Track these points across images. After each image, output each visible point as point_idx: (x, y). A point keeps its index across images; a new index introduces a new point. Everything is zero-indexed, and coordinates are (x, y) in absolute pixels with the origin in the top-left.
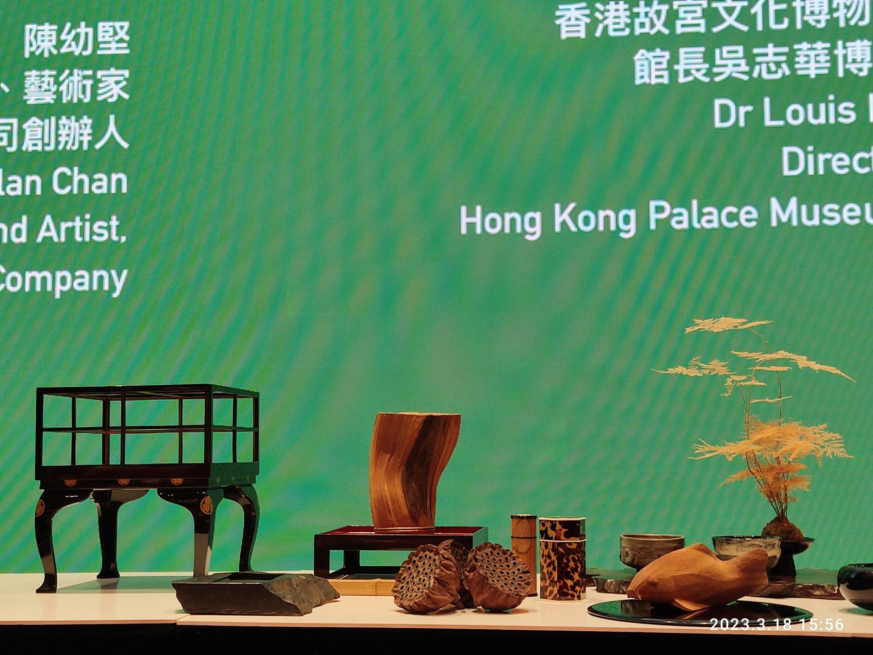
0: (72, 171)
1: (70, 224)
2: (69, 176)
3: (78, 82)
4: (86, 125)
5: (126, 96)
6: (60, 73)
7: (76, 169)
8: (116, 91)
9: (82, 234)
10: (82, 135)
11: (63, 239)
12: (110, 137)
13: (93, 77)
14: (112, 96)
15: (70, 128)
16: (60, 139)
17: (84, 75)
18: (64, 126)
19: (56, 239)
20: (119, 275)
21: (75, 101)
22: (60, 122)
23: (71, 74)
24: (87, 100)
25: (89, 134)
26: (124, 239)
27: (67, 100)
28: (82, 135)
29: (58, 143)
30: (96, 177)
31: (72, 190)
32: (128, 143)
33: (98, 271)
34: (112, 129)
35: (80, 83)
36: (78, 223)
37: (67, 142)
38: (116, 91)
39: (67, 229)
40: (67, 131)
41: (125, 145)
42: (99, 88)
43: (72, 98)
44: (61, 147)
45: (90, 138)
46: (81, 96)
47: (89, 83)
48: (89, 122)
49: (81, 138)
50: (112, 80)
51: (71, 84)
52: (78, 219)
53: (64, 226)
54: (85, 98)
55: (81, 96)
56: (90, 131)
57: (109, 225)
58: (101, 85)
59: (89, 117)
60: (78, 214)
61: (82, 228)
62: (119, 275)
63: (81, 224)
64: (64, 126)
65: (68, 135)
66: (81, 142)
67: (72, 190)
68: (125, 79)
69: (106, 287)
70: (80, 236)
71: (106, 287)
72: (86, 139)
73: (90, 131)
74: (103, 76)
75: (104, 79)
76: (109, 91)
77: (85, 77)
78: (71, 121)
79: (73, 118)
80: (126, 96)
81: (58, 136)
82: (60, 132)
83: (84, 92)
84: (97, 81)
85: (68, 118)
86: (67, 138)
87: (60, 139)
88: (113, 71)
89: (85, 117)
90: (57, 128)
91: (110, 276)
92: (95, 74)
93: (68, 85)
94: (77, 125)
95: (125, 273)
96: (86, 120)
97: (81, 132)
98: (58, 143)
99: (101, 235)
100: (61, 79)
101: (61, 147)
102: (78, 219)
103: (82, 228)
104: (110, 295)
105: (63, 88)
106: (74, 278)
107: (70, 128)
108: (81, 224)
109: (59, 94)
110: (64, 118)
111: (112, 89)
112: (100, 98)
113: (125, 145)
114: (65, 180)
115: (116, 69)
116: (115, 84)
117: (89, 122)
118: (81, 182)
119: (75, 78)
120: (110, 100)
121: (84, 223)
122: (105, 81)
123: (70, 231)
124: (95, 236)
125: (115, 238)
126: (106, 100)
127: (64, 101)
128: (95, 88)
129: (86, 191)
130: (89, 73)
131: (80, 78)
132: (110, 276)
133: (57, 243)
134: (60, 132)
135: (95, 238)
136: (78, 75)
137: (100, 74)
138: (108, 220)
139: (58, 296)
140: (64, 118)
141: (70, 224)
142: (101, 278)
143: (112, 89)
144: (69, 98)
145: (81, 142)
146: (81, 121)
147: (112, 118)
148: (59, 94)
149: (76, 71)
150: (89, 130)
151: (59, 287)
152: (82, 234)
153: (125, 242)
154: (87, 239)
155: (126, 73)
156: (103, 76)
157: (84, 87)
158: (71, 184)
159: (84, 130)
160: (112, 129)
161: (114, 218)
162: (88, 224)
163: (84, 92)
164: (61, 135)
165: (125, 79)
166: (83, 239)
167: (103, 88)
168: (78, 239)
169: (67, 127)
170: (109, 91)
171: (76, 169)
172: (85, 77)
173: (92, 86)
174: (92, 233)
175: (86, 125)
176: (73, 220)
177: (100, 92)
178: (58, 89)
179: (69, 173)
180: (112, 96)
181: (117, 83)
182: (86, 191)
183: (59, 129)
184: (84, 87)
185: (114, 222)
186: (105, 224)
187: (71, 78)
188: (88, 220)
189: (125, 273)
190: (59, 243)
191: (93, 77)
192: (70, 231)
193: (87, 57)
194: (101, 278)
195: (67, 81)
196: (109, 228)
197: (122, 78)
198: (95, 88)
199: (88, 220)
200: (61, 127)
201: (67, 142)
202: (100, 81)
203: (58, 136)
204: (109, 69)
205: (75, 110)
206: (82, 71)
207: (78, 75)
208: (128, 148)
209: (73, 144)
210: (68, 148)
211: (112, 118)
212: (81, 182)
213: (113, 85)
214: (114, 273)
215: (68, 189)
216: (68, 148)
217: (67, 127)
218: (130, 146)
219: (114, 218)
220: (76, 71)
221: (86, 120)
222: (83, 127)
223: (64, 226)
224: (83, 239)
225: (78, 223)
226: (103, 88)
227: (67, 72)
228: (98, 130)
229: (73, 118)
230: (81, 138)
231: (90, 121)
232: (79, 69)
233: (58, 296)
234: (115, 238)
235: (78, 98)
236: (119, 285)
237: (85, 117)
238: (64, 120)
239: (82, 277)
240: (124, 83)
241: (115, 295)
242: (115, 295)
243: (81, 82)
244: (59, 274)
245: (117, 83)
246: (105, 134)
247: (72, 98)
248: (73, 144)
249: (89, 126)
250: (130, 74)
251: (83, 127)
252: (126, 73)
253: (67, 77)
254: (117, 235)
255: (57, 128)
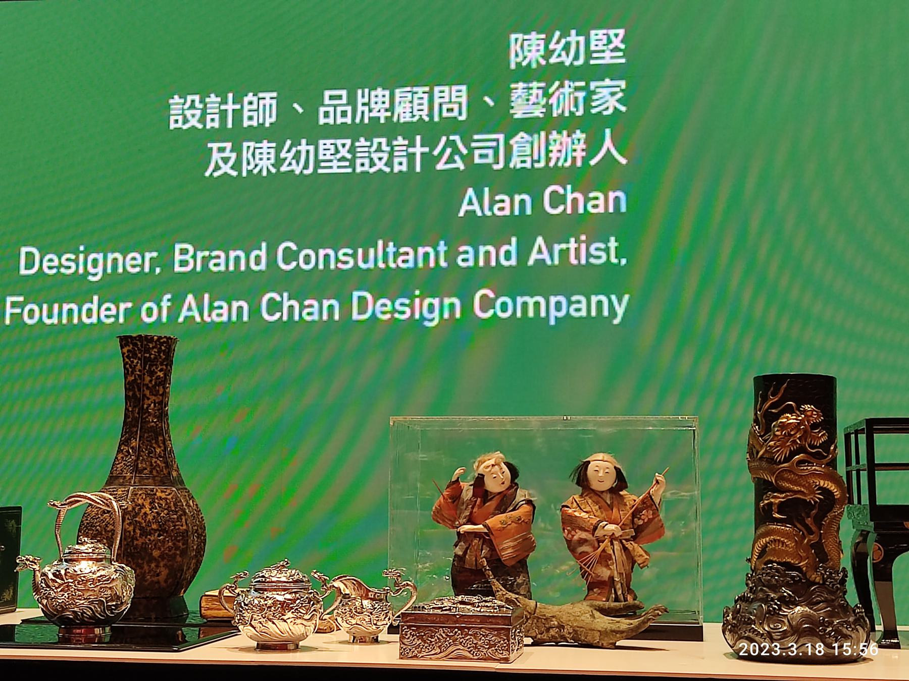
0: (565, 189)
1: (564, 246)
2: (562, 195)
3: (570, 94)
4: (579, 140)
5: (623, 109)
6: (549, 85)
7: (569, 187)
8: (612, 103)
9: (578, 257)
10: (575, 150)
11: (556, 262)
12: (606, 153)
13: (586, 88)
14: (607, 108)
15: (561, 143)
16: (551, 155)
17: (575, 86)
18: (555, 141)
19: (549, 262)
20: (620, 301)
21: (567, 114)
22: (550, 137)
23: (562, 86)
24: (580, 113)
25: (583, 150)
26: (624, 261)
27: (557, 114)
28: (575, 150)
29: (548, 160)
30: (592, 195)
31: (565, 210)
32: (627, 159)
33: (596, 296)
34: (608, 143)
35: (572, 96)
36: (572, 245)
37: (558, 159)
38: (612, 103)
39: (561, 251)
40: (558, 147)
41: (623, 161)
42: (593, 101)
43: (563, 112)
44: (552, 164)
45: (584, 154)
46: (573, 109)
47: (581, 95)
48: (583, 136)
49: (574, 154)
50: (606, 92)
51: (561, 97)
52: (572, 240)
53: (557, 248)
54: (577, 111)
55: (573, 109)
56: (584, 147)
57: (607, 246)
58: (594, 97)
59: (582, 132)
60: (572, 236)
61: (577, 250)
62: (620, 301)
63: (576, 245)
64: (555, 141)
65: (560, 151)
66: (574, 159)
67: (565, 210)
68: (622, 90)
69: (606, 313)
70: (576, 258)
71: (606, 313)
72: (579, 155)
73: (584, 147)
74: (597, 87)
75: (598, 90)
76: (604, 103)
77: (577, 89)
78: (563, 136)
79: (565, 133)
80: (623, 109)
81: (548, 152)
82: (550, 148)
83: (576, 106)
84: (590, 93)
85: (559, 132)
86: (559, 154)
87: (551, 155)
88: (608, 82)
89: (578, 132)
90: (548, 143)
91: (610, 301)
92: (588, 85)
93: (558, 98)
94: (569, 140)
95: (626, 298)
96: (578, 134)
97: (574, 147)
98: (548, 160)
99: (599, 257)
100: (551, 91)
101: (552, 164)
102: (572, 240)
103: (577, 250)
104: (611, 322)
105: (553, 101)
106: (570, 303)
107: (561, 143)
108: (576, 245)
109: (549, 107)
110: (554, 132)
111: (607, 101)
112: (594, 111)
113: (623, 161)
114: (557, 199)
115: (611, 80)
116: (610, 96)
117: (583, 136)
118: (575, 201)
119: (566, 90)
120: (605, 113)
121: (579, 245)
122: (598, 93)
123: (564, 253)
124: (592, 258)
125: (614, 260)
126: (600, 112)
127: (555, 115)
128: (588, 101)
129: (581, 211)
130: (583, 84)
131: (572, 90)
132: (610, 301)
133: (549, 266)
134: (550, 148)
135: (592, 260)
136: (570, 87)
137: (593, 85)
138: (607, 241)
139: (552, 322)
140: (554, 132)
141: (564, 246)
142: (600, 303)
143: (607, 101)
144: (560, 111)
145: (574, 159)
146: (574, 136)
147: (608, 132)
148: (549, 107)
149: (567, 83)
150: (582, 145)
151: (553, 312)
152: (578, 257)
153: (625, 265)
154: (583, 261)
155: (623, 84)
156: (597, 87)
157: (576, 99)
158: (564, 203)
159: (577, 145)
160: (608, 143)
161: (613, 239)
162: (583, 247)
163: (576, 106)
164: (552, 151)
165: (622, 90)
166: (579, 262)
167: (597, 100)
168: (574, 261)
169: (558, 142)
170: (604, 103)
171: (569, 187)
172: (577, 89)
173: (585, 98)
174: (589, 255)
175: (579, 140)
176: (568, 242)
177: (594, 104)
178: (547, 102)
179: (561, 191)
180: (607, 108)
181: (613, 94)
182: (581, 210)
183: (550, 144)
184: (576, 99)
185: (613, 244)
186: (602, 246)
187: (561, 90)
188: (583, 242)
189: (626, 298)
190: (553, 266)
191: (586, 88)
192: (564, 253)
193: (578, 67)
194: (600, 303)
195: (557, 94)
196: (607, 250)
197: (618, 89)
198: (588, 101)
199: (583, 242)
200: (552, 142)
201: (558, 159)
202: (594, 93)
203: (548, 152)
204: (603, 80)
205: (567, 124)
206: (573, 82)
207: (570, 87)
208: (627, 164)
209: (566, 160)
210: (560, 164)
211: (608, 132)
212: (575, 201)
213: (608, 97)
214: (613, 297)
215: (561, 208)
216: (560, 164)
217: (558, 142)
218: (628, 162)
219: (613, 239)
220: (567, 83)
221: (578, 134)
222: (576, 142)
223: (557, 248)
224: (579, 262)
225: (572, 245)
226: (597, 100)
227: (557, 84)
228: (593, 145)
229: (565, 133)
230: (574, 154)
231: (584, 136)
232: (570, 80)
233: (552, 322)
234: (614, 260)
235: (570, 111)
236: (620, 311)
237: (578, 132)
238: (554, 135)
239: (579, 302)
240: (620, 95)
241: (616, 321)
242: (616, 321)
243: (573, 94)
244: (553, 300)
245: (613, 94)
246: (601, 149)
247: (563, 112)
248: (566, 160)
249: (582, 141)
250: (627, 84)
251: (576, 142)
252: (623, 84)
253: (557, 89)
254: (616, 257)
255: (548, 143)
